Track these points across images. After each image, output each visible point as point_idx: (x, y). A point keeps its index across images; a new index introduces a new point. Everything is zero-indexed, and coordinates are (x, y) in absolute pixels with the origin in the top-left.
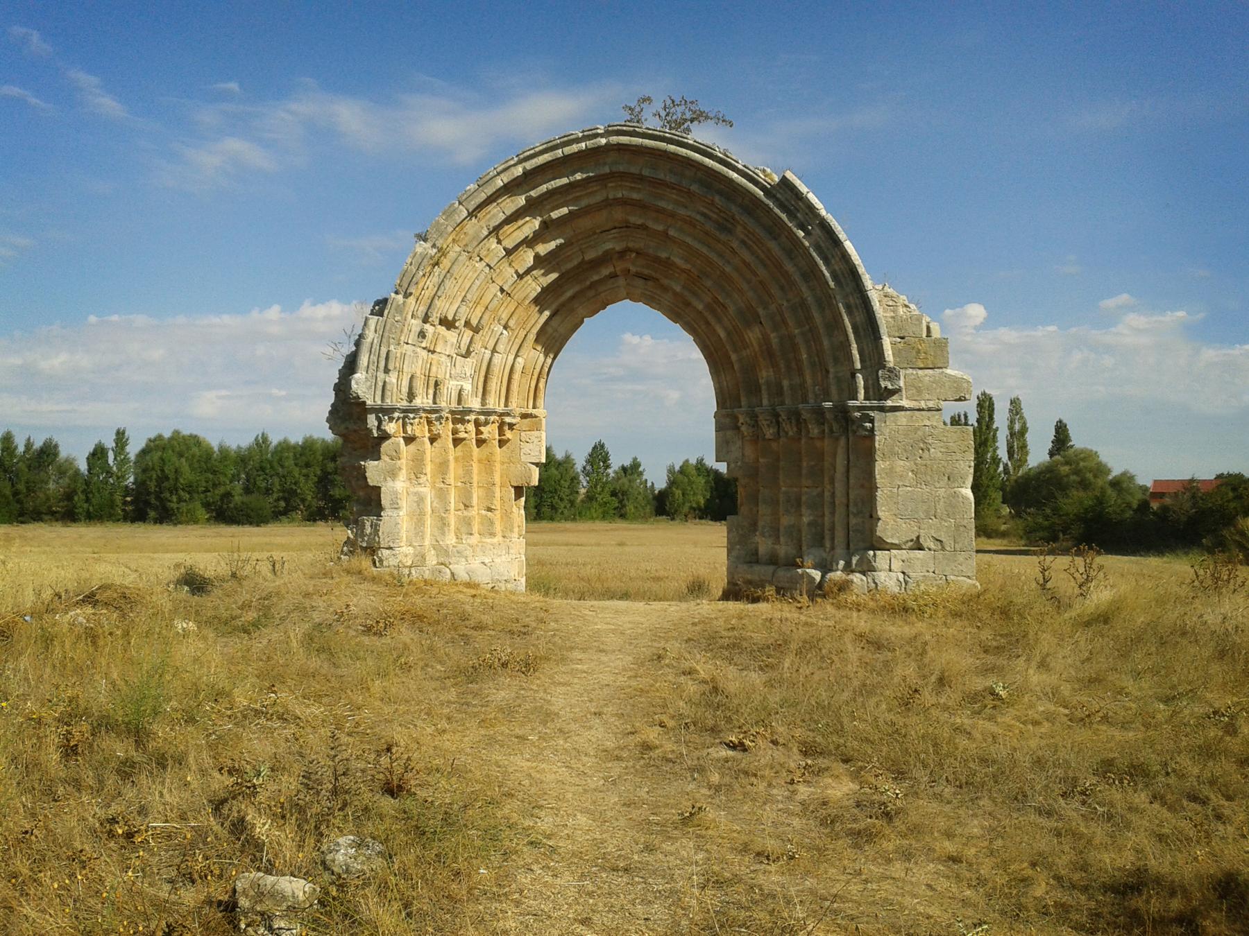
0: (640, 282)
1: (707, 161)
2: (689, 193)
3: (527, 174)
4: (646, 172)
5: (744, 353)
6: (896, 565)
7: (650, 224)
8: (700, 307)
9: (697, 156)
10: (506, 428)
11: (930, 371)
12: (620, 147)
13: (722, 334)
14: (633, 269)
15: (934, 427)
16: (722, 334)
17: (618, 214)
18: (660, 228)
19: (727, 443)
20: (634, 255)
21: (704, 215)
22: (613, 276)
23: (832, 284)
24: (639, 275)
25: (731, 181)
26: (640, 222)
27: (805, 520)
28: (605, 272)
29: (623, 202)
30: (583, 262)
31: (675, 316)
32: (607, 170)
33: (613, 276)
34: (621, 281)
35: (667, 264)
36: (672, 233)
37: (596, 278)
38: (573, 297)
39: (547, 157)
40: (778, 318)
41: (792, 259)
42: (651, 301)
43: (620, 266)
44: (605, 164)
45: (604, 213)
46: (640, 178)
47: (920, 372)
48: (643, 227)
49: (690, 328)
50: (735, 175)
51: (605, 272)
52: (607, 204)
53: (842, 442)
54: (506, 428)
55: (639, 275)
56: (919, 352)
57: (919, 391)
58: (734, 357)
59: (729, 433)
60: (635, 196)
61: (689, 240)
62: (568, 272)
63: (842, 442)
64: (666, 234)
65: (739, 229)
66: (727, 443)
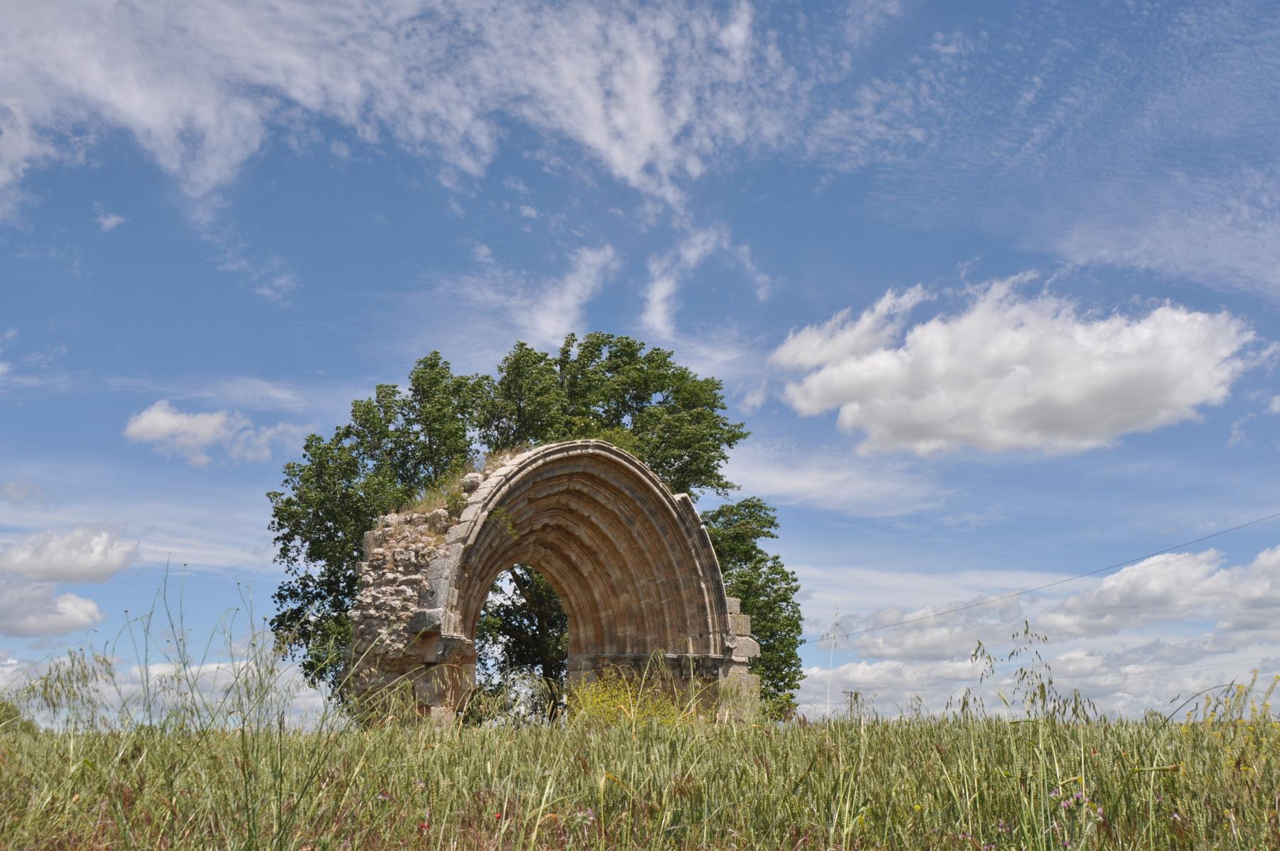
0: (543, 550)
16: (597, 597)
18: (587, 514)
21: (620, 510)
23: (700, 572)
32: (581, 470)
45: (556, 498)
58: (603, 614)
60: (586, 490)
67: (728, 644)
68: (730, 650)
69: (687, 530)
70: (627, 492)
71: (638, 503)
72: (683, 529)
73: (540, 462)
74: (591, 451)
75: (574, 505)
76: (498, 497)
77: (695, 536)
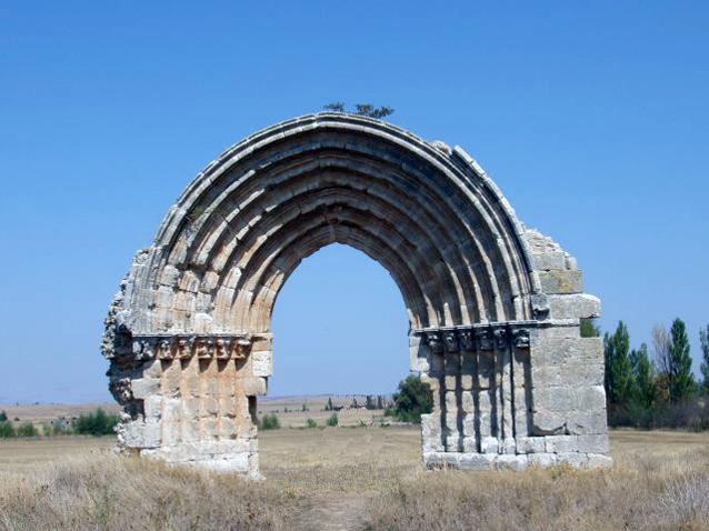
0: (345, 230)
1: (395, 139)
2: (383, 162)
3: (256, 151)
4: (349, 147)
6: (550, 447)
7: (354, 185)
8: (395, 247)
9: (388, 136)
11: (570, 296)
12: (328, 129)
14: (341, 218)
15: (574, 339)
17: (328, 178)
18: (361, 187)
20: (340, 208)
22: (325, 224)
24: (344, 223)
25: (414, 153)
26: (344, 183)
28: (318, 221)
29: (333, 169)
30: (300, 215)
31: (375, 255)
33: (325, 224)
34: (331, 229)
35: (367, 215)
37: (311, 226)
38: (293, 243)
42: (356, 244)
43: (331, 216)
44: (317, 142)
46: (344, 151)
47: (562, 297)
48: (348, 187)
49: (387, 264)
50: (417, 150)
51: (318, 221)
52: (320, 171)
53: (507, 352)
55: (344, 223)
56: (560, 281)
57: (562, 311)
60: (341, 164)
61: (384, 197)
62: (289, 223)
63: (507, 352)
64: (365, 191)
65: (422, 188)
67: (535, 307)
68: (545, 314)
70: (386, 157)
71: (404, 166)
73: (250, 149)
74: (315, 125)
76: (196, 194)
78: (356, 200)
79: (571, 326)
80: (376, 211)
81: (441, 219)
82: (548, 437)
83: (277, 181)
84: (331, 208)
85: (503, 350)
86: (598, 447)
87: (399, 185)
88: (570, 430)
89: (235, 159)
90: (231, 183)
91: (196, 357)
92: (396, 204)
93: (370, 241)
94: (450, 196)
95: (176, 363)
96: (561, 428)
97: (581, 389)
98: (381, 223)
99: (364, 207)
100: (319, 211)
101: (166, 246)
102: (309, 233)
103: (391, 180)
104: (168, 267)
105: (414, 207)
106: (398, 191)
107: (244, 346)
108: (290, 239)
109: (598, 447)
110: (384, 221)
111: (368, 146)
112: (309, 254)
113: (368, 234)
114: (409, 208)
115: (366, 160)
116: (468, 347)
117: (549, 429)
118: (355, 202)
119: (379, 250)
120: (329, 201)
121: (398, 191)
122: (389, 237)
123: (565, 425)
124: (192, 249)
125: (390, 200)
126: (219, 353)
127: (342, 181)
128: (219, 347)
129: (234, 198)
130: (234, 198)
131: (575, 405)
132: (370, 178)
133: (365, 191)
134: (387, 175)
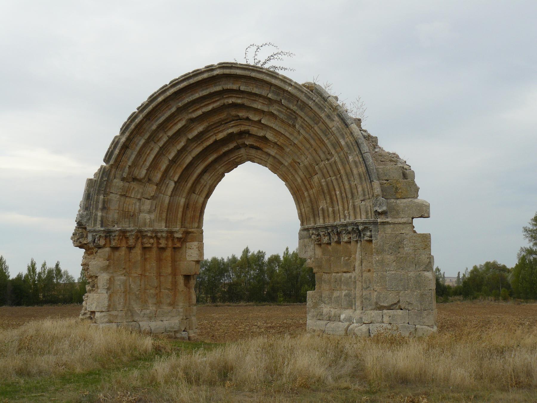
3: (175, 93)
4: (242, 88)
5: (311, 192)
6: (386, 319)
7: (251, 117)
10: (176, 240)
11: (404, 201)
13: (299, 180)
18: (256, 119)
19: (305, 246)
21: (279, 111)
24: (252, 147)
27: (344, 293)
28: (232, 146)
31: (274, 170)
33: (237, 148)
34: (243, 151)
35: (264, 139)
36: (263, 122)
37: (226, 149)
39: (185, 84)
40: (325, 171)
41: (326, 135)
43: (240, 141)
44: (220, 85)
49: (284, 178)
51: (232, 146)
53: (359, 244)
54: (176, 240)
55: (252, 147)
56: (397, 188)
57: (398, 213)
59: (306, 240)
60: (239, 101)
64: (260, 121)
65: (299, 119)
66: (305, 246)
69: (329, 116)
72: (323, 115)
75: (242, 114)
76: (132, 126)
77: (336, 119)
78: (255, 129)
79: (404, 223)
80: (270, 136)
81: (312, 142)
82: (385, 311)
83: (194, 115)
84: (241, 134)
85: (357, 241)
86: (425, 320)
87: (282, 116)
88: (402, 307)
89: (160, 99)
90: (160, 118)
91: (139, 245)
92: (282, 131)
93: (271, 160)
94: (317, 124)
95: (123, 251)
96: (395, 304)
97: (412, 274)
98: (276, 147)
99: (261, 134)
100: (230, 137)
101: (112, 165)
102: (225, 154)
103: (275, 112)
104: (115, 180)
105: (296, 134)
106: (283, 121)
107: (177, 238)
108: (211, 159)
109: (425, 320)
110: (276, 143)
111: (256, 87)
112: (228, 171)
113: (269, 155)
114: (291, 134)
115: (257, 98)
116: (335, 240)
117: (386, 305)
118: (254, 130)
119: (276, 167)
120: (235, 130)
121: (283, 121)
122: (282, 157)
123: (399, 302)
124: (135, 164)
125: (277, 128)
126: (158, 243)
127: (242, 114)
128: (158, 239)
129: (162, 127)
130: (162, 127)
131: (406, 287)
132: (263, 112)
133: (260, 121)
134: (274, 109)
